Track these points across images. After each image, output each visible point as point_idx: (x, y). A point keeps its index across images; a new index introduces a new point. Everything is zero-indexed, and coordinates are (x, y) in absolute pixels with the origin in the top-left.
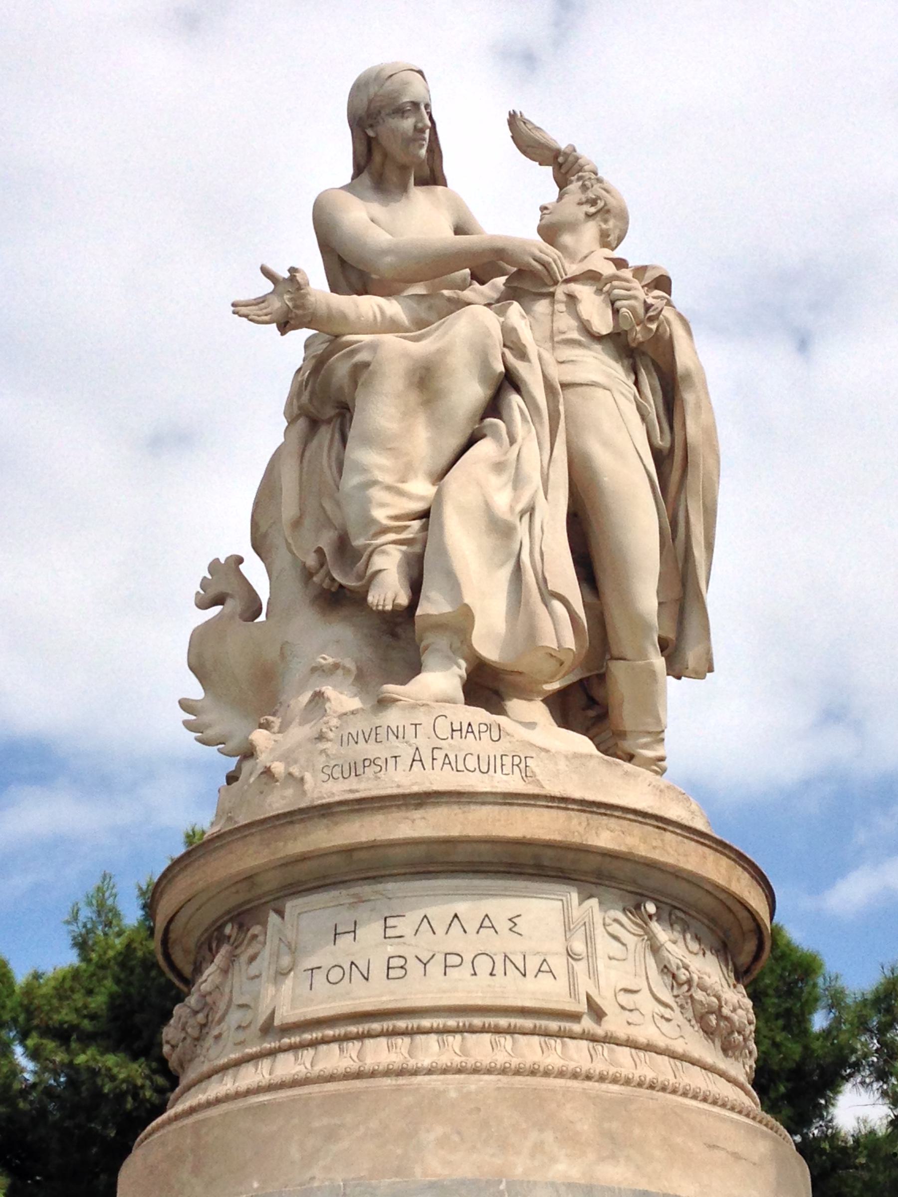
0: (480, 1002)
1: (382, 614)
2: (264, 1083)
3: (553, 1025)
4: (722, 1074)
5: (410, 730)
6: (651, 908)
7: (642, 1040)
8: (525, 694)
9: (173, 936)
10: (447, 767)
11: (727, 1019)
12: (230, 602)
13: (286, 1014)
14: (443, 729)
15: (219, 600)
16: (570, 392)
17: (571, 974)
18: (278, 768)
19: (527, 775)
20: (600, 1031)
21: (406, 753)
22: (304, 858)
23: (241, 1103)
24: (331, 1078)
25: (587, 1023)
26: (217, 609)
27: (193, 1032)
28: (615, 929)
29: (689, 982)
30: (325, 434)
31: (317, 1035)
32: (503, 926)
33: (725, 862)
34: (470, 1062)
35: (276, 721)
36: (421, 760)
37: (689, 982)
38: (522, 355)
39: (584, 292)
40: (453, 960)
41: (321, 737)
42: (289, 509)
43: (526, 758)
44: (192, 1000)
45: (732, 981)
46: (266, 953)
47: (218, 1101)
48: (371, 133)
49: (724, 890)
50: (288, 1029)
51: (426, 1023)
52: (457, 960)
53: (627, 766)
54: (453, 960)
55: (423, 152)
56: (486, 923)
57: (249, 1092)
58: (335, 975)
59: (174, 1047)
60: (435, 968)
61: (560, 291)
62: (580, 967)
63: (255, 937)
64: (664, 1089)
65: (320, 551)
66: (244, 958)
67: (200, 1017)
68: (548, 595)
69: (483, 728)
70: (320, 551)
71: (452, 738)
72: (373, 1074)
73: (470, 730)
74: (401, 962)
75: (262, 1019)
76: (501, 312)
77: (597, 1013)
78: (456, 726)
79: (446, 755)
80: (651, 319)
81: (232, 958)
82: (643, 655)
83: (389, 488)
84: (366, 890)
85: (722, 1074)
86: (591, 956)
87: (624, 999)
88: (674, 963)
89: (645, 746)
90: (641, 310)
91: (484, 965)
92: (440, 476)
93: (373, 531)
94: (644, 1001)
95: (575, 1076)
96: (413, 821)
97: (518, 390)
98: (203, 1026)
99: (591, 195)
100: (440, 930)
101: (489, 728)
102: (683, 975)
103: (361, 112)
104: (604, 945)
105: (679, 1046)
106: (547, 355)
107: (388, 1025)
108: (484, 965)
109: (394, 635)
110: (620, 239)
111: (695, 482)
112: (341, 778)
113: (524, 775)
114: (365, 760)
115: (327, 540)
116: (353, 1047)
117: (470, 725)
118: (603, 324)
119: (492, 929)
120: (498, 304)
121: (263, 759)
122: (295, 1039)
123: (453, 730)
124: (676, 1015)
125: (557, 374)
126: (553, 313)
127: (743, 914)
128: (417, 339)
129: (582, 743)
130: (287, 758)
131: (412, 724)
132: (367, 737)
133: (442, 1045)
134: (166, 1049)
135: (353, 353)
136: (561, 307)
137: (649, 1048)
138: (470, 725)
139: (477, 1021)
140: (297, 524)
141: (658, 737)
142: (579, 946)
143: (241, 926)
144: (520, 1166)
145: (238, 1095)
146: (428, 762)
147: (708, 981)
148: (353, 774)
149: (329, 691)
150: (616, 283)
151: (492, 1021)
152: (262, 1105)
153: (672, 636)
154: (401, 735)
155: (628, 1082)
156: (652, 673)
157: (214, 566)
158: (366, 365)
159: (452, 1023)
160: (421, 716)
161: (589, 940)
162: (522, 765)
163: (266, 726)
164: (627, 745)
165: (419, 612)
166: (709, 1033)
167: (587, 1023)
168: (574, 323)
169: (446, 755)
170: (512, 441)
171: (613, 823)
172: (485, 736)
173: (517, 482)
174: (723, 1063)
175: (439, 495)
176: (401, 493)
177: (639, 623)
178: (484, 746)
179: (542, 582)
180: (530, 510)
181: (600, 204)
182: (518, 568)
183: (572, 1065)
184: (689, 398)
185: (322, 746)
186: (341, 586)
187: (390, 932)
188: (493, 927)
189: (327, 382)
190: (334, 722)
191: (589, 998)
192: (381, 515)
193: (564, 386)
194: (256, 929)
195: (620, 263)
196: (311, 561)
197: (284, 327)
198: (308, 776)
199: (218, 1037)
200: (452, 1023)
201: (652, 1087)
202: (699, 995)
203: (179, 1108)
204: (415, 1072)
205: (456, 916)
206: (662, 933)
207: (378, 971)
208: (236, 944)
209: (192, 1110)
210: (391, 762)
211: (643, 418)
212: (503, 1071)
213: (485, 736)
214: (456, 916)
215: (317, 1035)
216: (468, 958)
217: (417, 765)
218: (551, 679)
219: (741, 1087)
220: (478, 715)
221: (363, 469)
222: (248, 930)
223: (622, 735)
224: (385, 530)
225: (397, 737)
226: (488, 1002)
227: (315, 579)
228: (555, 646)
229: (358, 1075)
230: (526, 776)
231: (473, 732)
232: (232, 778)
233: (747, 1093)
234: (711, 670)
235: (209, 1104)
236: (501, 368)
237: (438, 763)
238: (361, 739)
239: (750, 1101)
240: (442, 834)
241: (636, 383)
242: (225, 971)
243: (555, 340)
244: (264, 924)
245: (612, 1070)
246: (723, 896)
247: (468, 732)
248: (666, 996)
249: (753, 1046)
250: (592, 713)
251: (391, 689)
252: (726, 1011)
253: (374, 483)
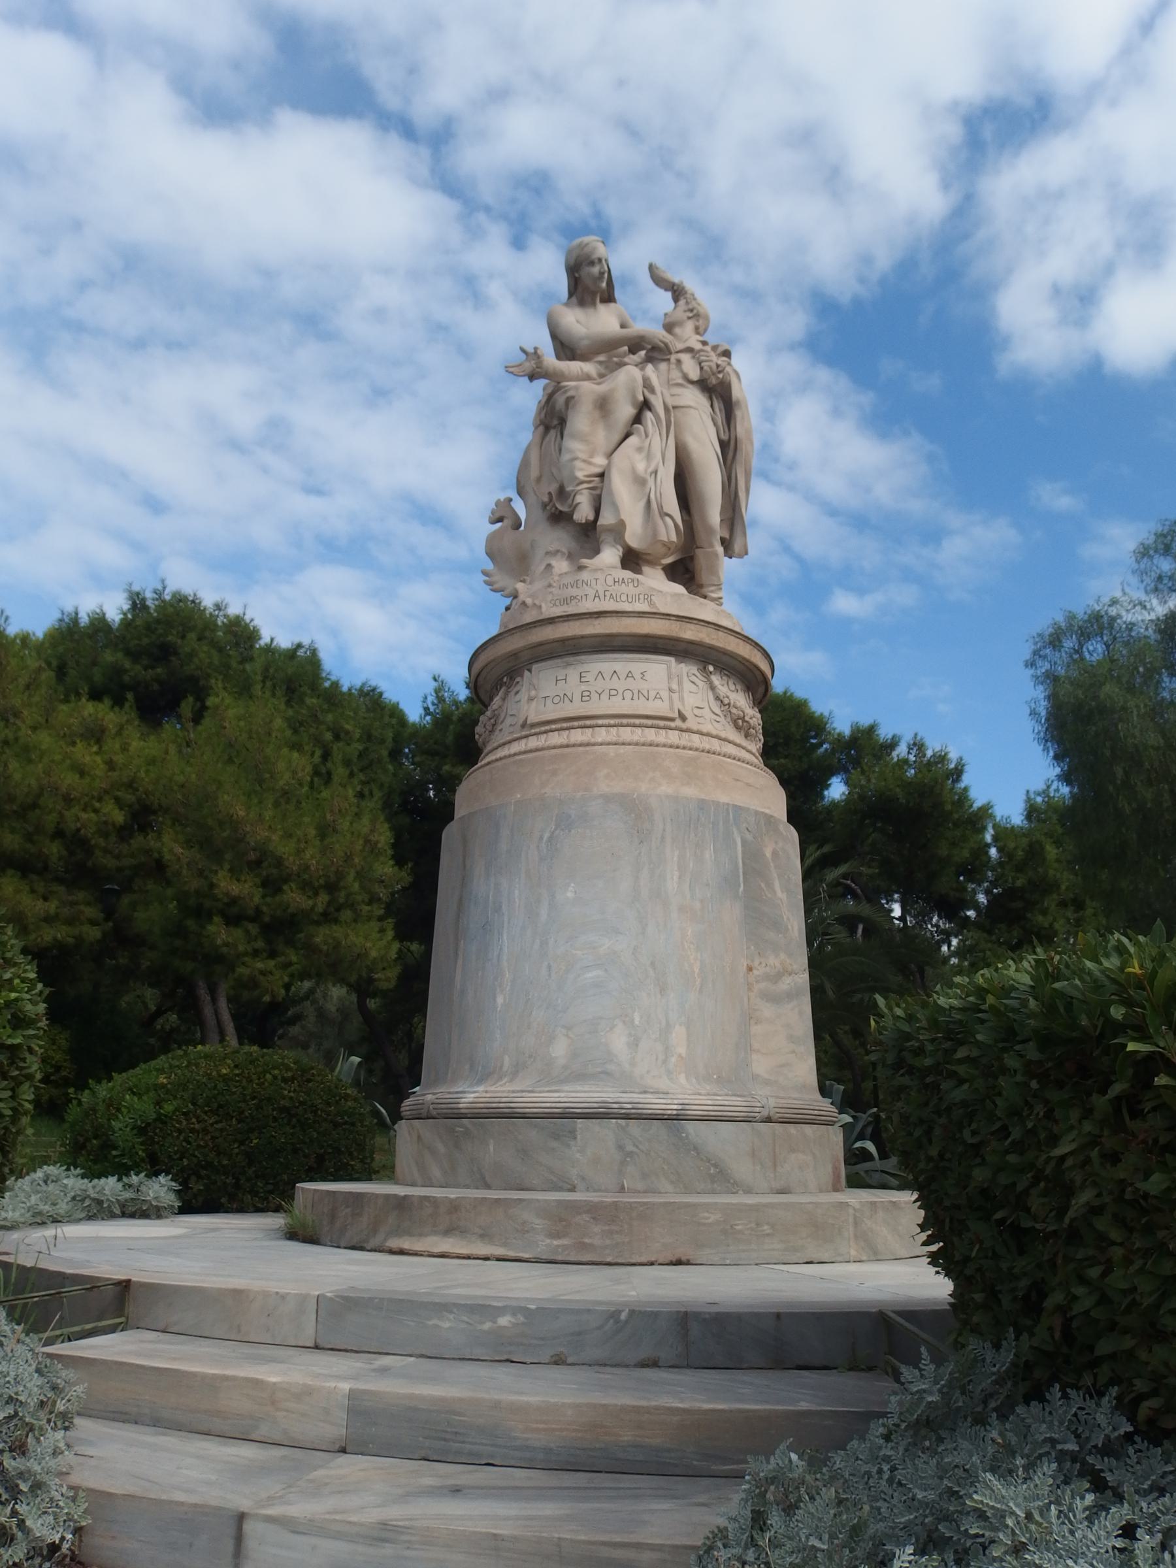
0: (626, 712)
1: (581, 524)
2: (523, 750)
3: (662, 723)
4: (744, 748)
5: (594, 582)
6: (711, 668)
7: (705, 731)
8: (652, 563)
9: (478, 684)
11: (747, 722)
12: (506, 521)
13: (533, 718)
14: (610, 581)
15: (500, 520)
16: (676, 410)
17: (671, 699)
18: (529, 601)
19: (651, 603)
20: (684, 726)
21: (592, 593)
22: (541, 644)
23: (511, 759)
24: (554, 747)
25: (678, 723)
26: (499, 525)
27: (489, 728)
28: (693, 678)
29: (729, 704)
30: (552, 433)
31: (547, 728)
32: (637, 676)
33: (748, 647)
34: (621, 740)
35: (528, 579)
37: (729, 704)
38: (652, 391)
39: (686, 358)
40: (613, 692)
41: (550, 586)
42: (534, 472)
44: (488, 713)
45: (751, 705)
46: (524, 689)
47: (501, 759)
48: (577, 275)
49: (748, 661)
50: (533, 726)
51: (600, 722)
52: (615, 693)
53: (702, 600)
54: (613, 692)
55: (604, 285)
56: (629, 675)
57: (515, 754)
58: (556, 700)
59: (480, 736)
60: (605, 696)
61: (673, 358)
62: (675, 696)
63: (518, 682)
64: (714, 753)
65: (550, 494)
66: (513, 693)
67: (492, 721)
68: (664, 515)
70: (550, 494)
72: (574, 745)
74: (588, 693)
75: (521, 722)
76: (642, 369)
77: (683, 718)
80: (720, 372)
81: (507, 694)
82: (712, 546)
83: (584, 461)
84: (571, 659)
85: (744, 748)
86: (681, 691)
87: (697, 711)
88: (722, 695)
89: (712, 592)
90: (714, 367)
91: (628, 695)
92: (610, 455)
93: (577, 482)
94: (706, 712)
95: (671, 747)
97: (650, 410)
98: (494, 725)
99: (690, 307)
100: (607, 679)
101: (633, 581)
102: (726, 701)
103: (572, 262)
104: (687, 686)
105: (723, 735)
106: (665, 391)
107: (581, 723)
108: (628, 695)
109: (587, 536)
110: (705, 330)
111: (741, 457)
115: (553, 488)
116: (565, 733)
118: (694, 375)
120: (641, 365)
121: (521, 597)
122: (537, 730)
124: (722, 719)
125: (671, 402)
126: (669, 370)
127: (757, 673)
128: (599, 384)
129: (680, 589)
130: (533, 596)
133: (608, 732)
134: (477, 736)
135: (566, 392)
136: (673, 366)
137: (708, 735)
139: (625, 721)
140: (539, 480)
141: (719, 586)
142: (675, 686)
143: (511, 678)
144: (644, 788)
145: (510, 756)
147: (738, 704)
149: (554, 563)
150: (702, 353)
151: (632, 721)
152: (521, 760)
153: (727, 536)
155: (697, 750)
156: (716, 555)
157: (498, 503)
158: (573, 397)
159: (612, 722)
160: (599, 575)
161: (680, 684)
162: (648, 598)
163: (524, 581)
164: (705, 591)
165: (599, 523)
166: (738, 728)
167: (678, 723)
168: (679, 374)
170: (647, 436)
171: (692, 626)
172: (631, 585)
173: (649, 457)
174: (745, 743)
175: (609, 465)
176: (590, 463)
177: (710, 531)
178: (630, 589)
179: (660, 508)
180: (656, 472)
181: (695, 312)
182: (649, 501)
183: (670, 742)
184: (738, 414)
185: (550, 590)
186: (561, 512)
187: (583, 680)
189: (553, 408)
190: (556, 578)
191: (679, 711)
192: (580, 475)
193: (674, 407)
194: (518, 679)
195: (704, 343)
196: (546, 499)
197: (532, 377)
198: (543, 605)
199: (501, 730)
200: (612, 722)
201: (708, 752)
202: (734, 711)
203: (483, 762)
204: (594, 745)
206: (716, 680)
207: (577, 697)
209: (489, 763)
210: (584, 597)
211: (715, 424)
212: (637, 744)
213: (631, 585)
215: (547, 728)
216: (620, 692)
217: (597, 599)
218: (665, 556)
219: (754, 754)
220: (628, 574)
221: (570, 451)
223: (701, 586)
224: (582, 482)
226: (630, 712)
227: (548, 508)
228: (665, 539)
229: (567, 746)
232: (507, 609)
233: (757, 758)
234: (746, 553)
235: (497, 760)
236: (641, 398)
237: (608, 598)
238: (569, 587)
239: (759, 761)
240: (608, 632)
241: (712, 406)
242: (504, 699)
243: (670, 384)
244: (522, 676)
245: (689, 744)
246: (747, 664)
248: (718, 711)
249: (761, 737)
250: (687, 576)
251: (585, 561)
252: (747, 718)
253: (576, 459)
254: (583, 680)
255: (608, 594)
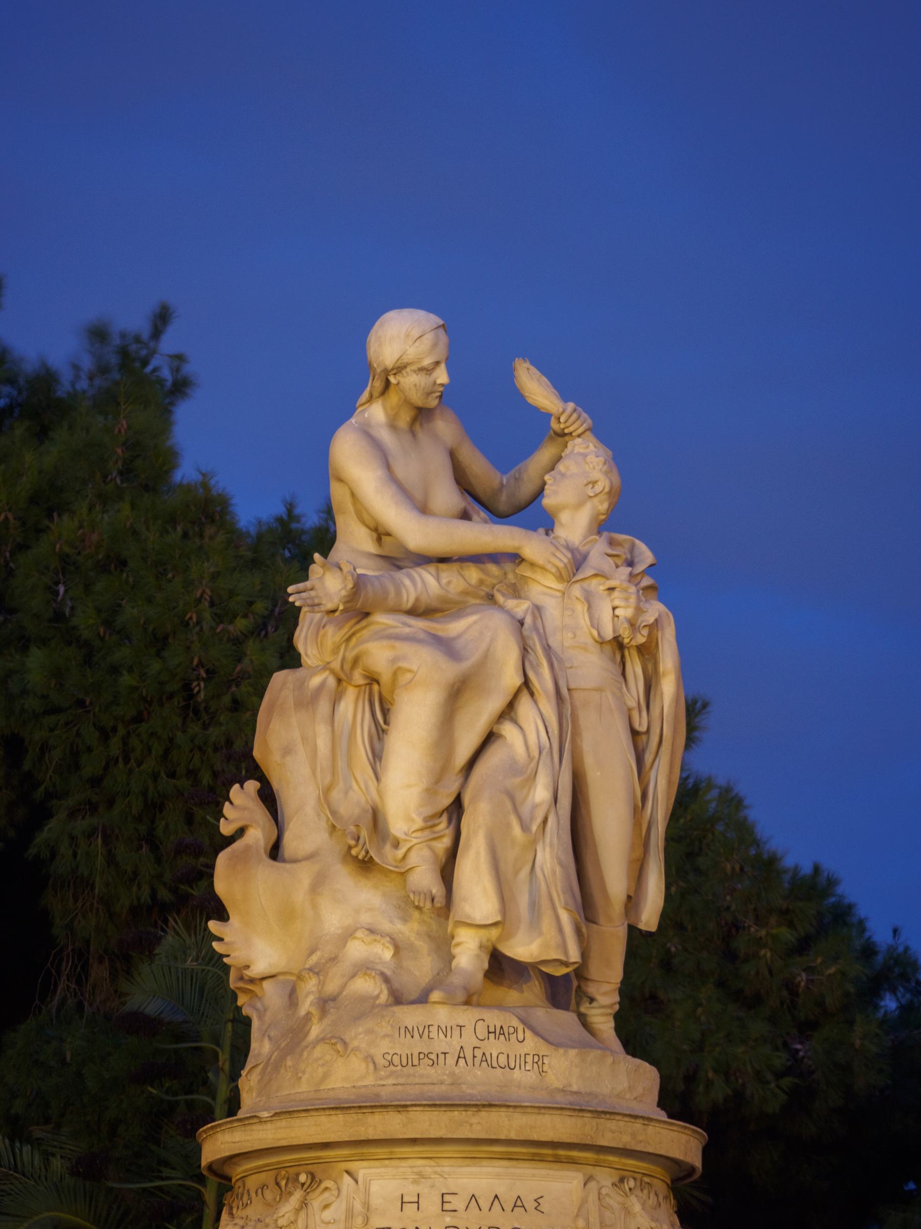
5: (456, 1032)
10: (484, 1064)
14: (482, 1032)
32: (530, 1205)
36: (465, 1058)
43: (543, 1056)
56: (518, 1203)
63: (326, 1189)
69: (512, 1030)
71: (488, 1039)
73: (502, 1032)
78: (492, 1029)
79: (484, 1054)
81: (304, 1204)
96: (471, 1125)
97: (532, 694)
112: (399, 1067)
113: (541, 1070)
114: (420, 1053)
117: (502, 1027)
119: (523, 1208)
123: (489, 1032)
131: (457, 1026)
132: (421, 1033)
138: (502, 1027)
146: (470, 1062)
148: (410, 1063)
154: (449, 1035)
169: (484, 1054)
172: (513, 1037)
187: (446, 1206)
188: (523, 1206)
194: (328, 1183)
205: (496, 1196)
208: (308, 1190)
210: (442, 1057)
214: (496, 1196)
217: (462, 1061)
222: (321, 1181)
225: (446, 1036)
230: (543, 1071)
231: (504, 1034)
237: (477, 1061)
247: (500, 1034)
254: (446, 1206)
255: (479, 1053)
